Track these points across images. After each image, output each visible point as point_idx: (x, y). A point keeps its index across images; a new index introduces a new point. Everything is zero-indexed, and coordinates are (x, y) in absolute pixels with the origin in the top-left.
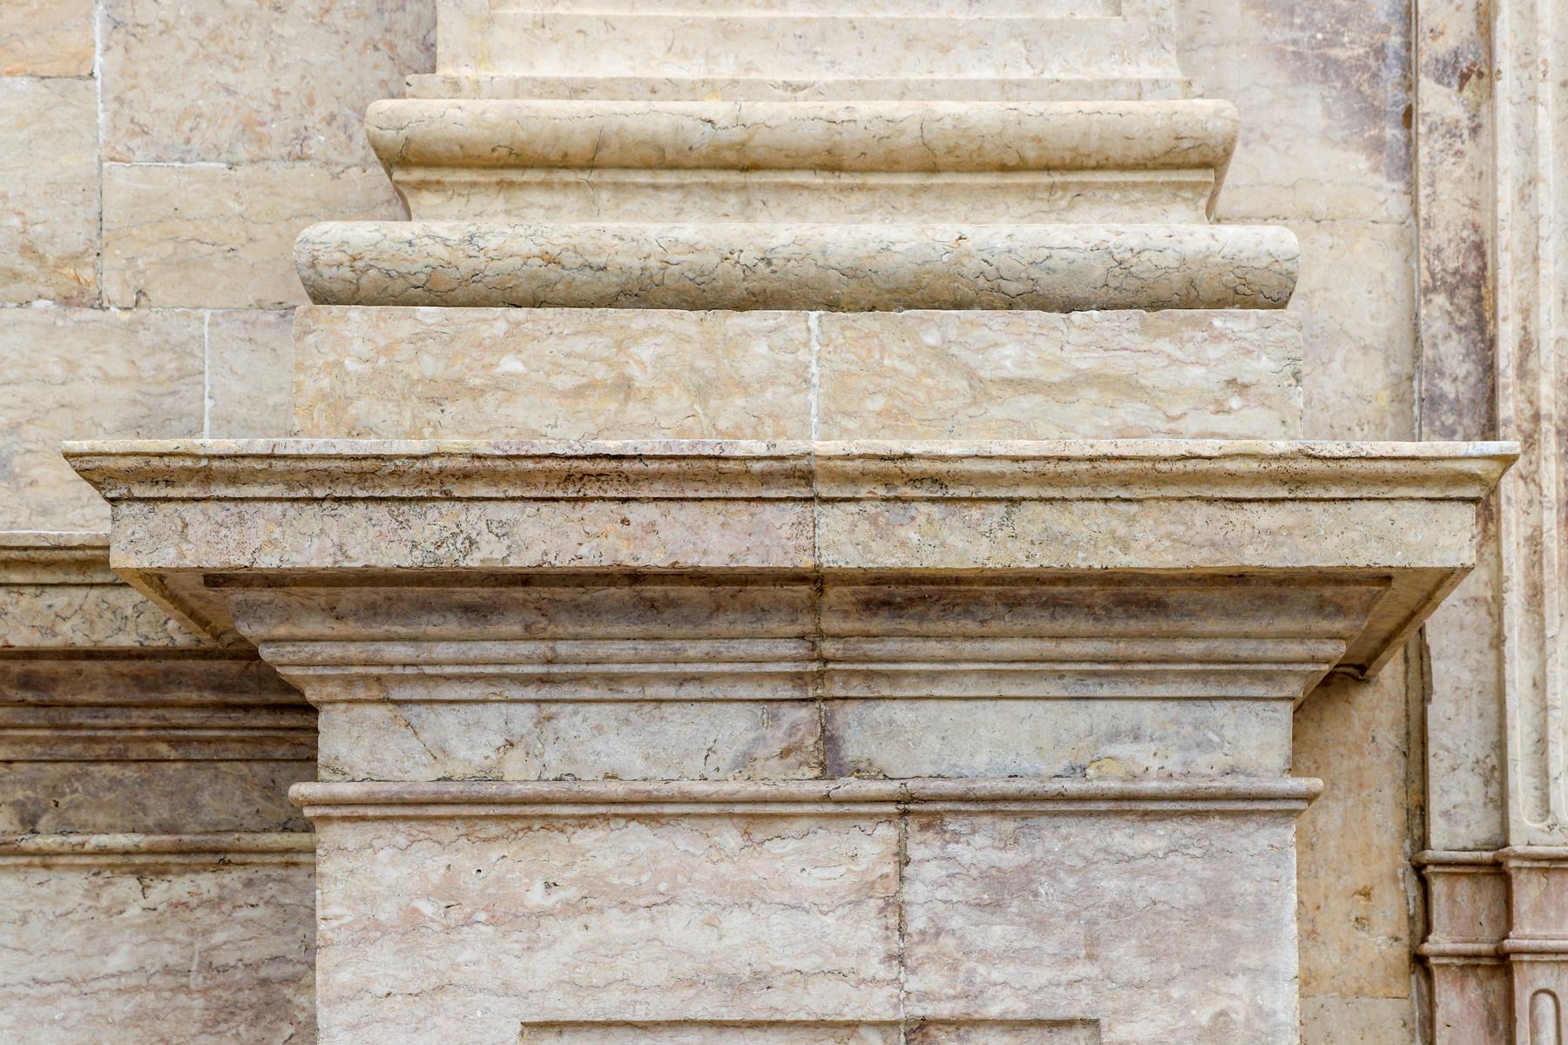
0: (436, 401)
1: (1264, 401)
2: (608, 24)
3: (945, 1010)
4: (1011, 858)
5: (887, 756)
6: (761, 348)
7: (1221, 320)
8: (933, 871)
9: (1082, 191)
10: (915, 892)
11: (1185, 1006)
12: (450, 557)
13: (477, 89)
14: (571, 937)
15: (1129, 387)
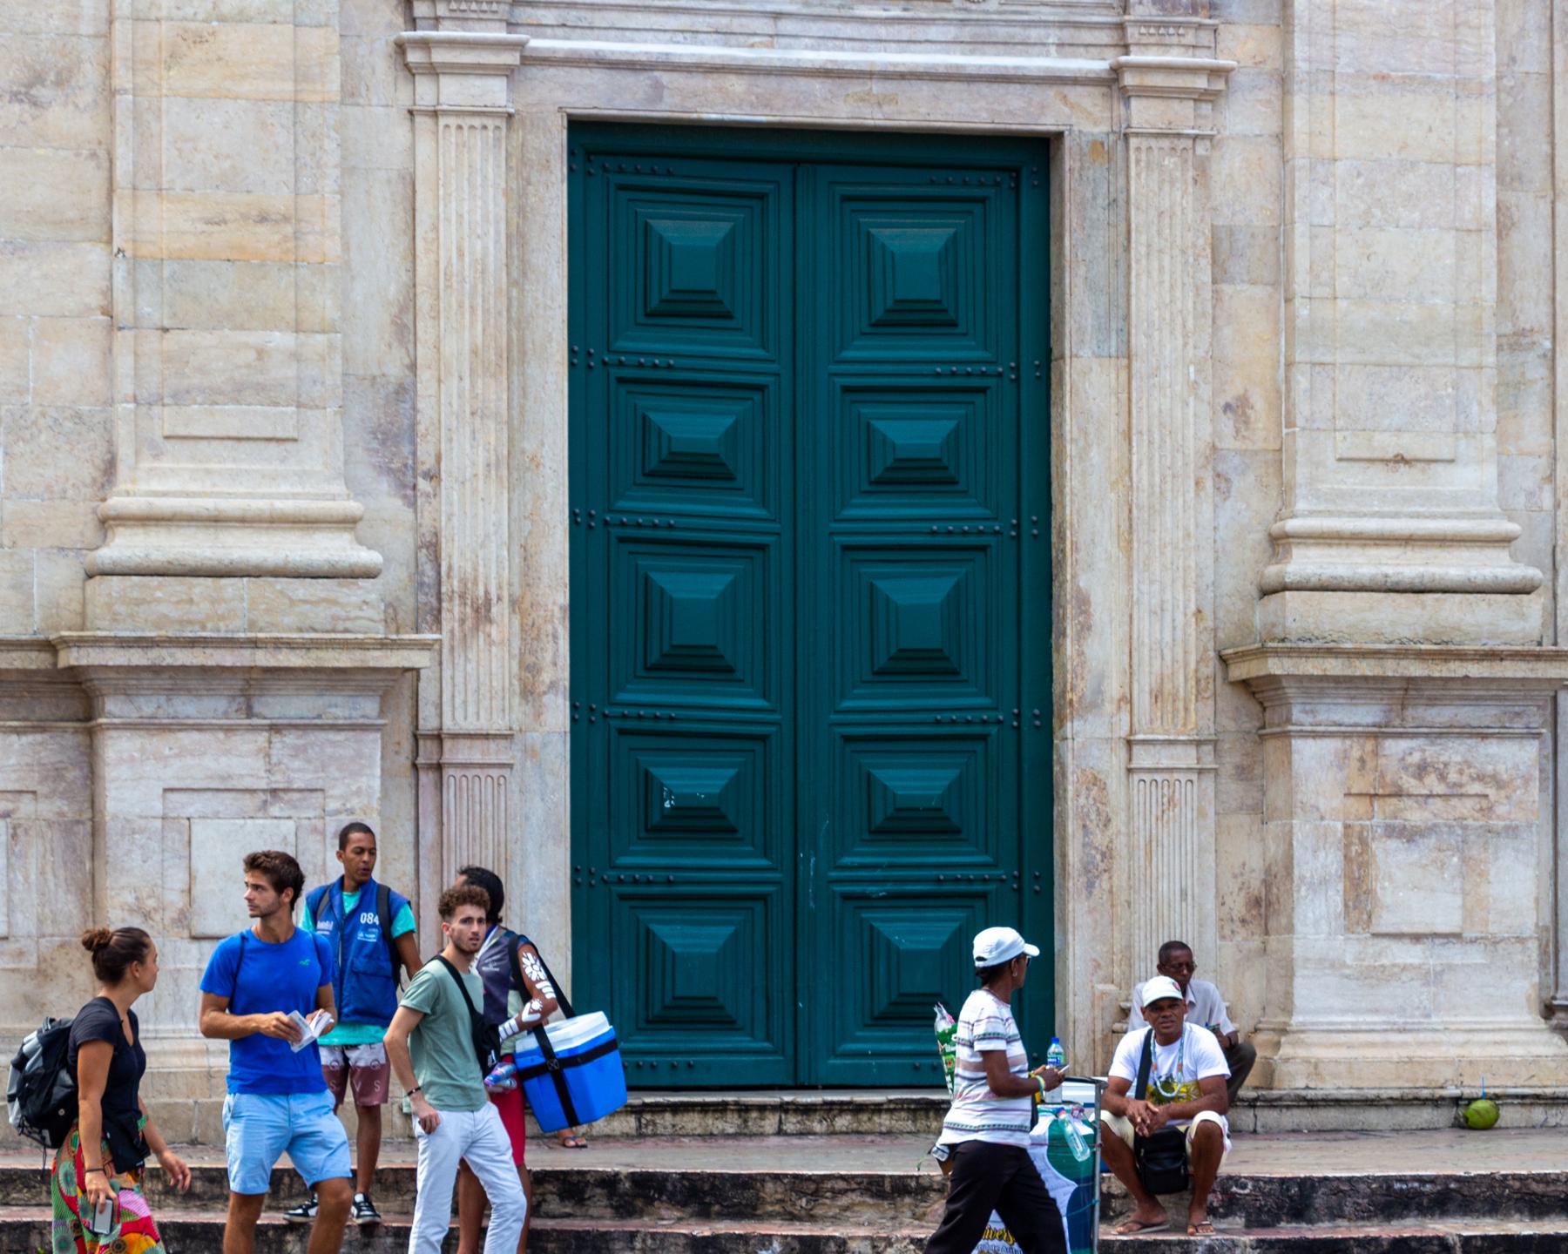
0: (137, 605)
1: (373, 607)
2: (172, 470)
3: (281, 786)
4: (301, 742)
5: (266, 712)
6: (230, 590)
7: (361, 582)
8: (279, 745)
9: (317, 529)
10: (273, 752)
11: (349, 785)
12: (157, 662)
13: (135, 495)
14: (176, 764)
15: (335, 602)
